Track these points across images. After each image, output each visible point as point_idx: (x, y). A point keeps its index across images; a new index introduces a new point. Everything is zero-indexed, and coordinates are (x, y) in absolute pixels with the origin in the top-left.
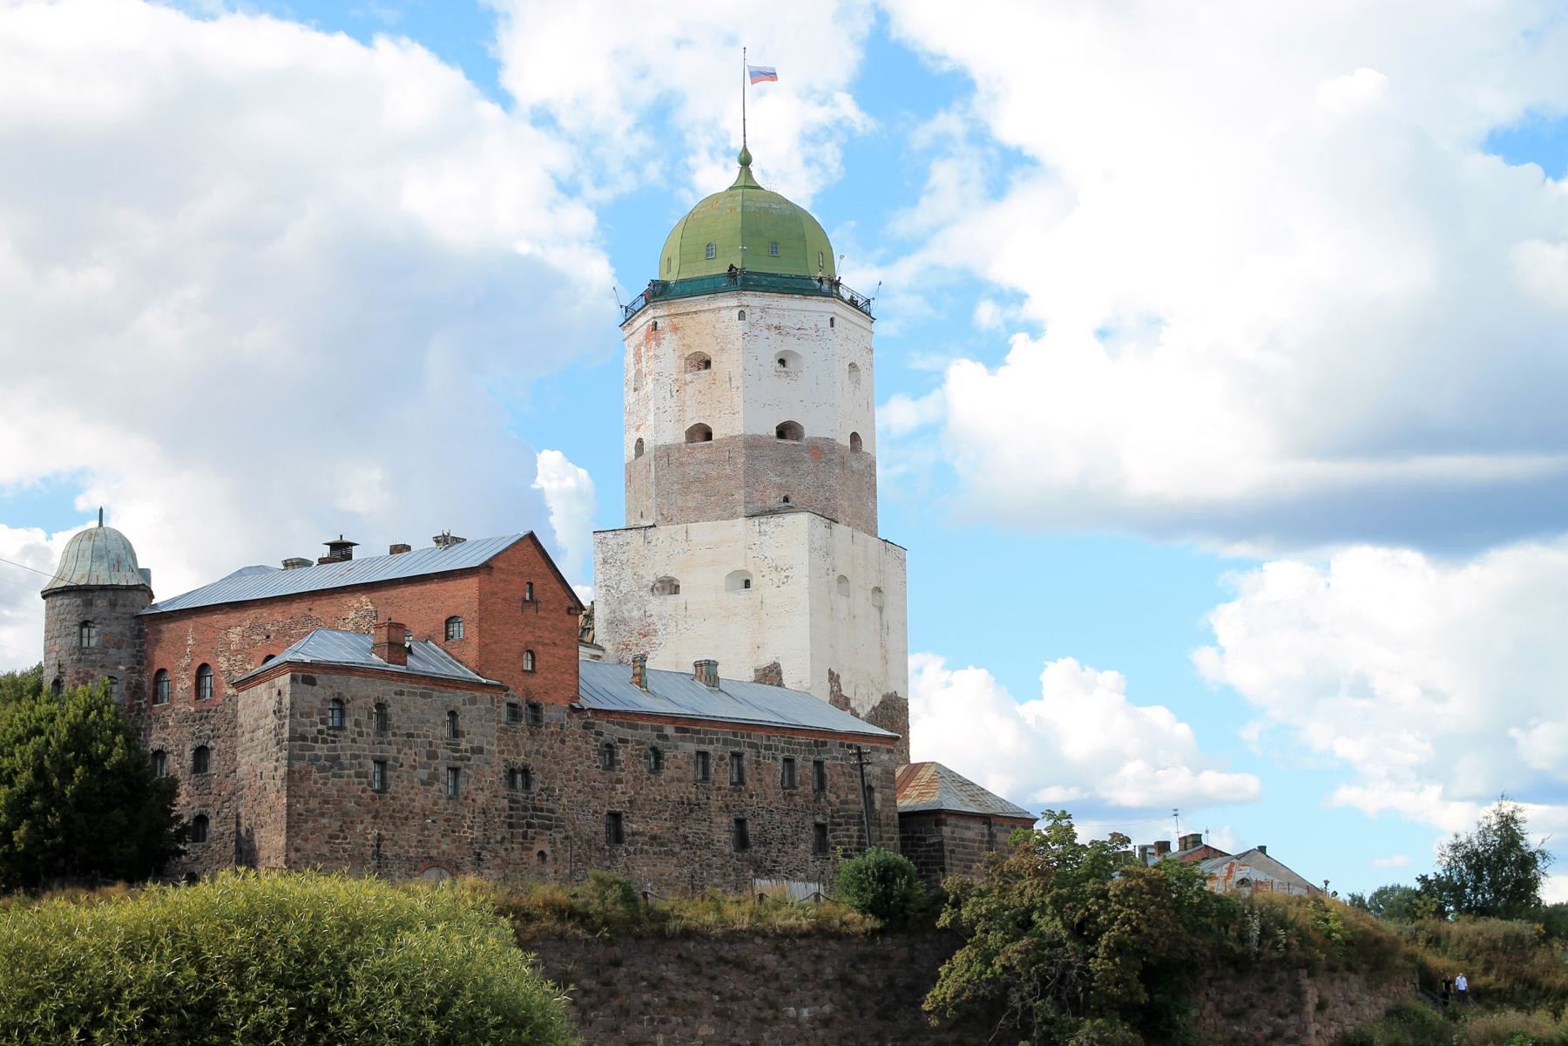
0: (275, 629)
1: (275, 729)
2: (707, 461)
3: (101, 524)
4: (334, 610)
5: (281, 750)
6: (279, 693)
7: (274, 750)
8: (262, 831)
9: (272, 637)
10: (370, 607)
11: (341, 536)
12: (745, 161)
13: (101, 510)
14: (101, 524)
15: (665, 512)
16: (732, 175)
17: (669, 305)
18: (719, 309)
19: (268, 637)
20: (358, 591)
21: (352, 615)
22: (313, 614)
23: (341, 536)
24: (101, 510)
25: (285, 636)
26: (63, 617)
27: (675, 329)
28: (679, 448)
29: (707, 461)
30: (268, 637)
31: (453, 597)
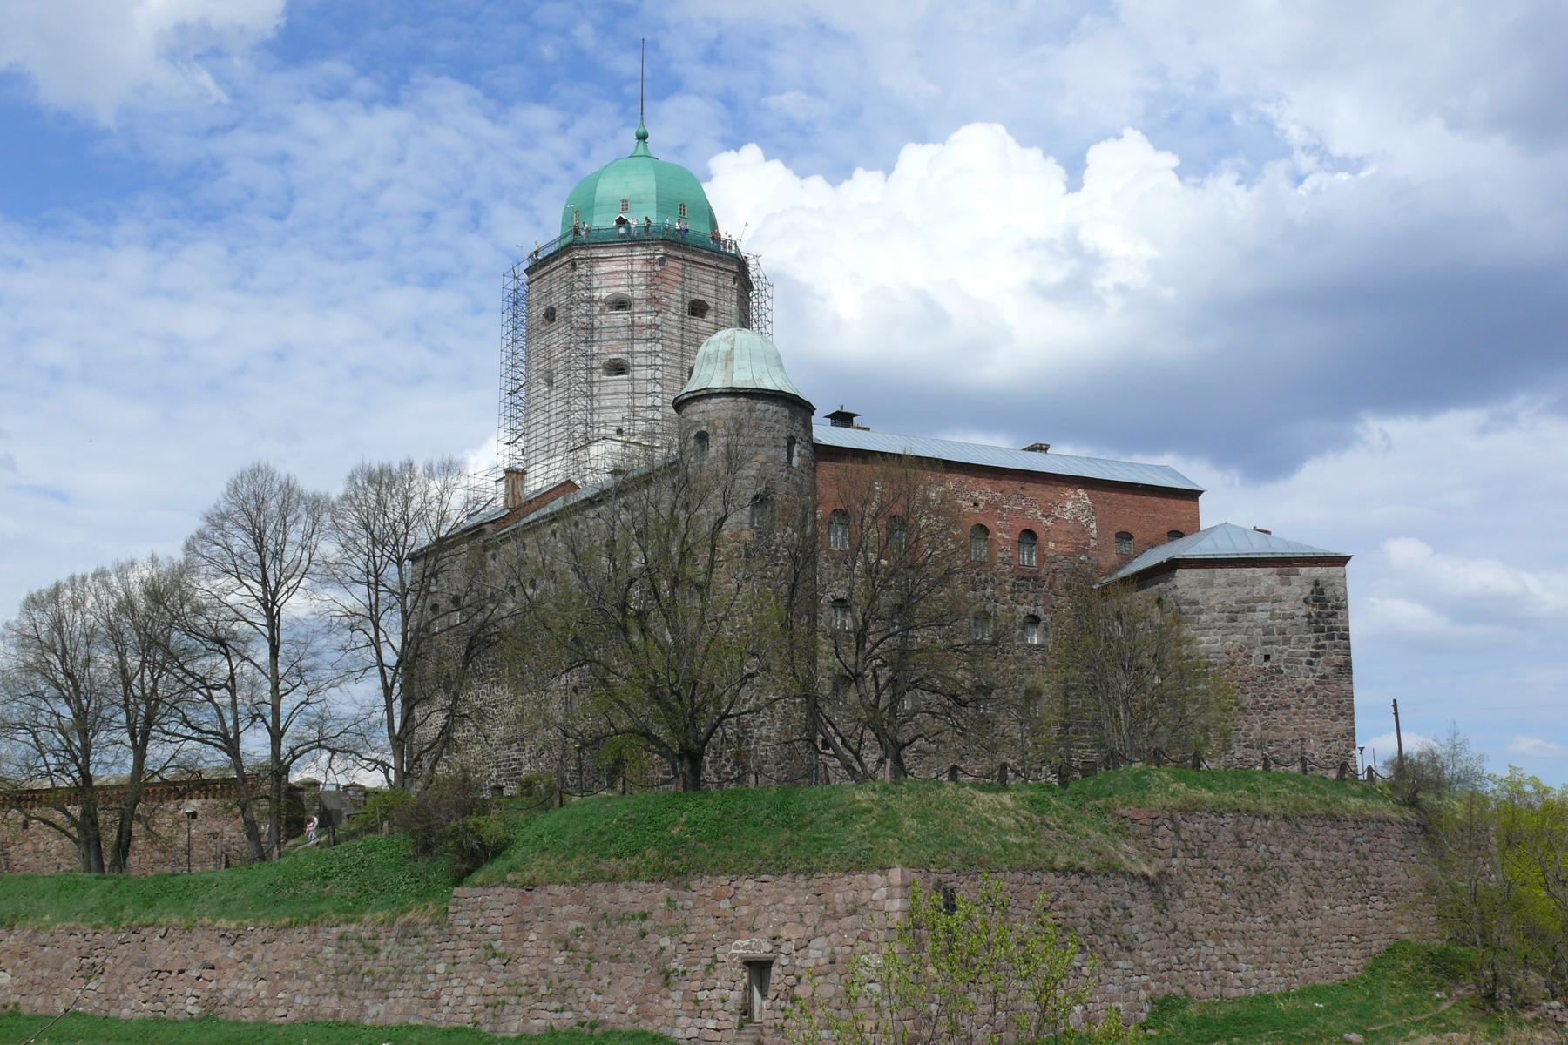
0: (984, 498)
1: (1309, 616)
4: (1050, 496)
5: (1332, 638)
6: (1316, 583)
7: (1310, 635)
8: (1273, 713)
9: (981, 507)
10: (1088, 502)
11: (842, 407)
19: (976, 505)
20: (1076, 483)
22: (1026, 493)
23: (842, 407)
25: (996, 509)
26: (770, 424)
30: (976, 505)
31: (1174, 512)
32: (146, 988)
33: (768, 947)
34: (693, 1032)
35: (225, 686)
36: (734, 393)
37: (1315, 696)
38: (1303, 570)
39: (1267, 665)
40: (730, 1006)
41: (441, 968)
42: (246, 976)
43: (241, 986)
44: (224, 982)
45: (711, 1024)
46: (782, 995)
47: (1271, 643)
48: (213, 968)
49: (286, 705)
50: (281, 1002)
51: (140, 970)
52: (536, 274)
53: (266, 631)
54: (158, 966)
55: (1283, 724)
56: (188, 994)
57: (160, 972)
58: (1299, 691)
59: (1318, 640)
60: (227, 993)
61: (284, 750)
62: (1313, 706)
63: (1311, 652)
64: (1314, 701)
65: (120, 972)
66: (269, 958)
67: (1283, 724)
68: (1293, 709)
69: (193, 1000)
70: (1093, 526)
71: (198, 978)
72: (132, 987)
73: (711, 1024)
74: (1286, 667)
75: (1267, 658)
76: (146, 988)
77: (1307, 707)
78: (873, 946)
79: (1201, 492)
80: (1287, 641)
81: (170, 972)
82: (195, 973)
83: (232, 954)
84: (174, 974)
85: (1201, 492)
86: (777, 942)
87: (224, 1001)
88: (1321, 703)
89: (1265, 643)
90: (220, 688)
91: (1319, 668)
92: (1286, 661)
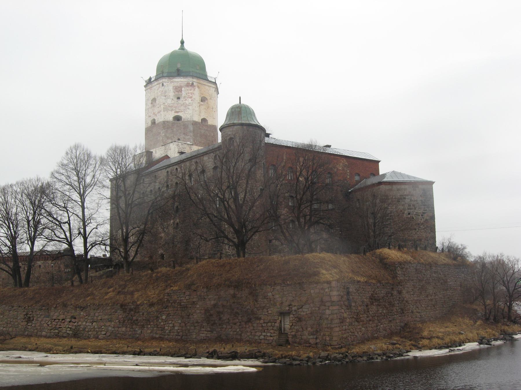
2: (207, 130)
3: (240, 103)
12: (182, 43)
13: (240, 98)
14: (240, 103)
15: (195, 141)
16: (179, 45)
17: (197, 79)
18: (210, 86)
21: (341, 164)
24: (240, 98)
27: (198, 87)
28: (199, 123)
29: (207, 130)
32: (51, 325)
33: (287, 308)
34: (262, 337)
35: (67, 222)
36: (242, 125)
37: (424, 226)
38: (420, 186)
39: (409, 216)
40: (275, 328)
41: (164, 317)
42: (89, 321)
43: (87, 324)
44: (80, 323)
45: (269, 334)
46: (294, 324)
47: (411, 209)
48: (75, 318)
49: (88, 229)
50: (103, 329)
51: (47, 319)
52: (148, 87)
53: (80, 203)
54: (54, 318)
55: (414, 235)
56: (67, 327)
57: (55, 320)
58: (419, 224)
59: (425, 208)
60: (82, 326)
61: (88, 245)
62: (423, 229)
63: (423, 212)
64: (424, 227)
65: (40, 319)
66: (97, 314)
67: (414, 235)
68: (417, 230)
69: (69, 329)
70: (348, 171)
71: (70, 322)
72: (45, 325)
73: (269, 334)
74: (415, 217)
75: (409, 214)
76: (51, 325)
77: (421, 230)
78: (327, 308)
79: (379, 161)
80: (415, 209)
81: (59, 320)
82: (68, 320)
83: (82, 313)
84: (60, 320)
85: (379, 161)
86: (291, 306)
87: (81, 329)
88: (425, 228)
89: (408, 209)
90: (65, 223)
91: (425, 217)
92: (415, 215)
